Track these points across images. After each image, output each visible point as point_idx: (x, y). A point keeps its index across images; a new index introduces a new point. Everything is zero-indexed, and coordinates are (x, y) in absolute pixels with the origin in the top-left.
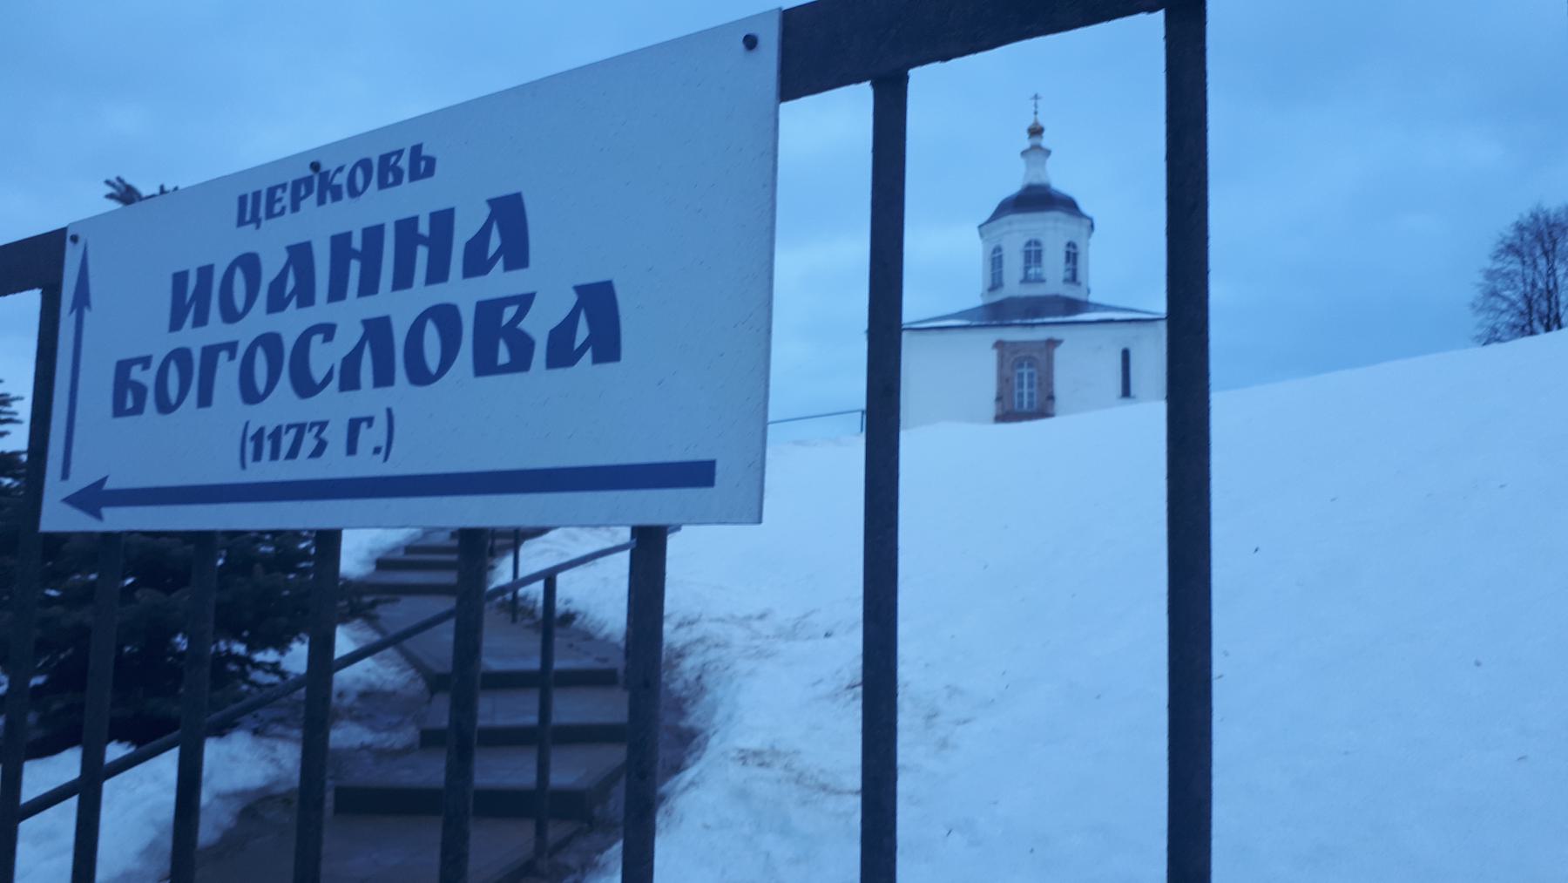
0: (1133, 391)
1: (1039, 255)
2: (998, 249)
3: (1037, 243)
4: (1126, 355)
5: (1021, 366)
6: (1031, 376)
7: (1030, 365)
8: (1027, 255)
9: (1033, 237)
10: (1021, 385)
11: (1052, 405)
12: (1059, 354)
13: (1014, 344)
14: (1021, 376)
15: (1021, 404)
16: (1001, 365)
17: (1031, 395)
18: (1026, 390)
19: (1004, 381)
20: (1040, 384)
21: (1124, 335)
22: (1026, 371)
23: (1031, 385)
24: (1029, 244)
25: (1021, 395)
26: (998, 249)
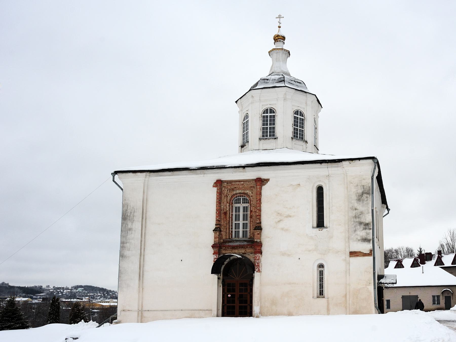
0: (326, 222)
1: (273, 119)
2: (247, 116)
3: (272, 111)
4: (320, 190)
5: (238, 202)
6: (245, 209)
7: (245, 201)
8: (265, 119)
9: (268, 107)
10: (237, 218)
11: (260, 234)
12: (266, 190)
13: (230, 182)
14: (238, 209)
15: (237, 233)
16: (219, 201)
17: (245, 226)
18: (241, 222)
19: (222, 214)
20: (251, 217)
21: (318, 174)
22: (241, 206)
23: (245, 218)
24: (266, 111)
25: (237, 226)
26: (247, 116)
